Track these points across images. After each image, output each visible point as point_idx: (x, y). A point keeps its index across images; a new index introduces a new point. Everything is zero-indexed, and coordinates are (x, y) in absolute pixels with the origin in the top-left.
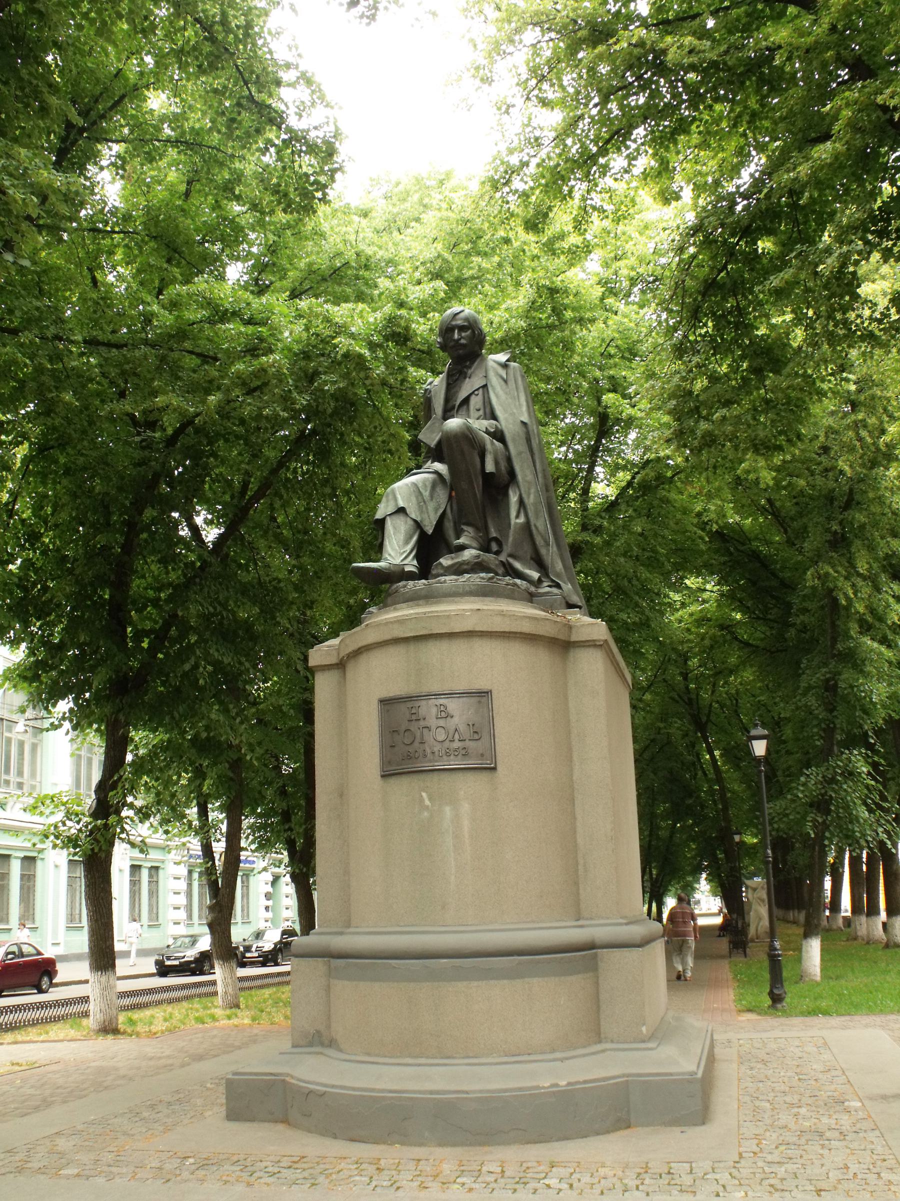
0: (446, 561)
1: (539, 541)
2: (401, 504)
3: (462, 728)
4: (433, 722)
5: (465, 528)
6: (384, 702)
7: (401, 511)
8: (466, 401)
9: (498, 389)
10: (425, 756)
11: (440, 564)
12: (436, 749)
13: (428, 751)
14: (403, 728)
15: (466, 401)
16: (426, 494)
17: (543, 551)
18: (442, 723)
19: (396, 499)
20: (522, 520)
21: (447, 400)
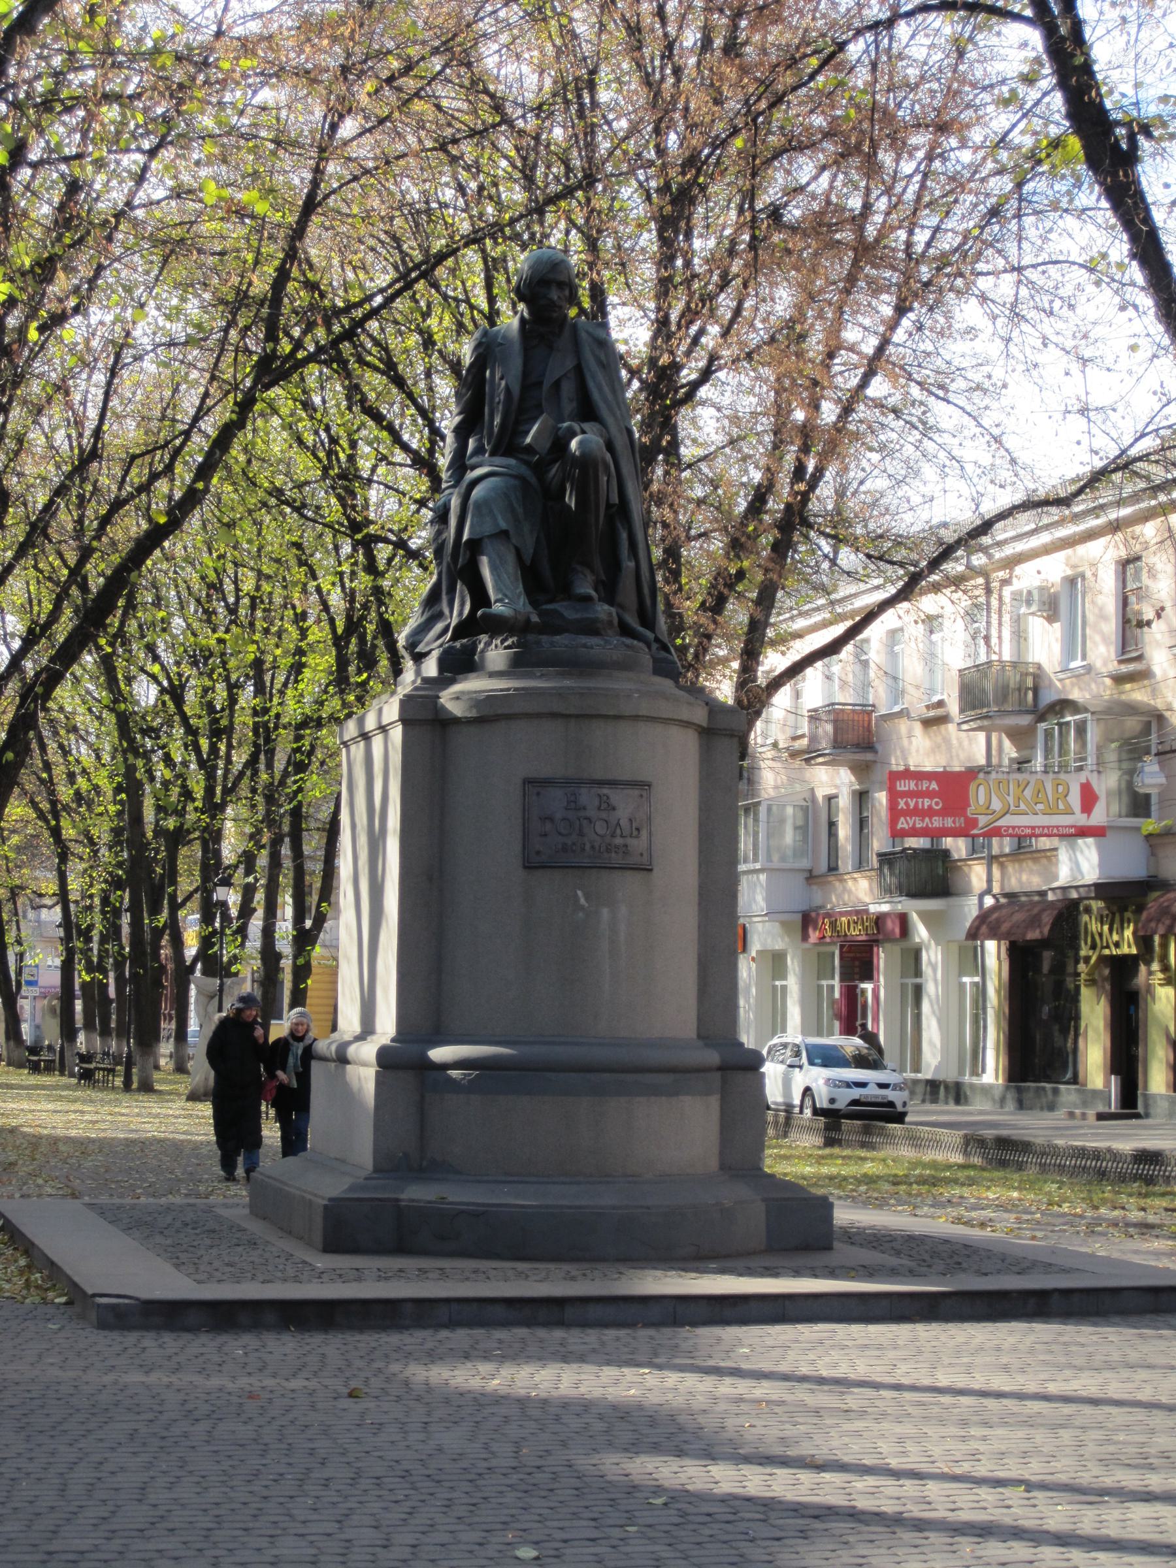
0: (569, 612)
1: (646, 591)
2: (503, 525)
3: (624, 823)
4: (591, 812)
5: (579, 568)
6: (528, 782)
7: (504, 534)
8: (557, 385)
9: (600, 376)
10: (583, 850)
11: (555, 611)
12: (597, 845)
13: (588, 847)
14: (558, 816)
15: (557, 385)
16: (520, 510)
17: (648, 601)
18: (604, 815)
19: (495, 519)
20: (632, 564)
21: (525, 374)
